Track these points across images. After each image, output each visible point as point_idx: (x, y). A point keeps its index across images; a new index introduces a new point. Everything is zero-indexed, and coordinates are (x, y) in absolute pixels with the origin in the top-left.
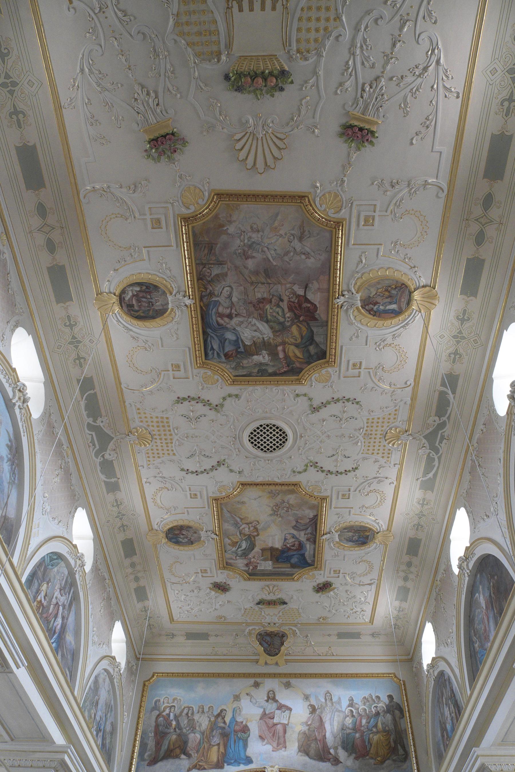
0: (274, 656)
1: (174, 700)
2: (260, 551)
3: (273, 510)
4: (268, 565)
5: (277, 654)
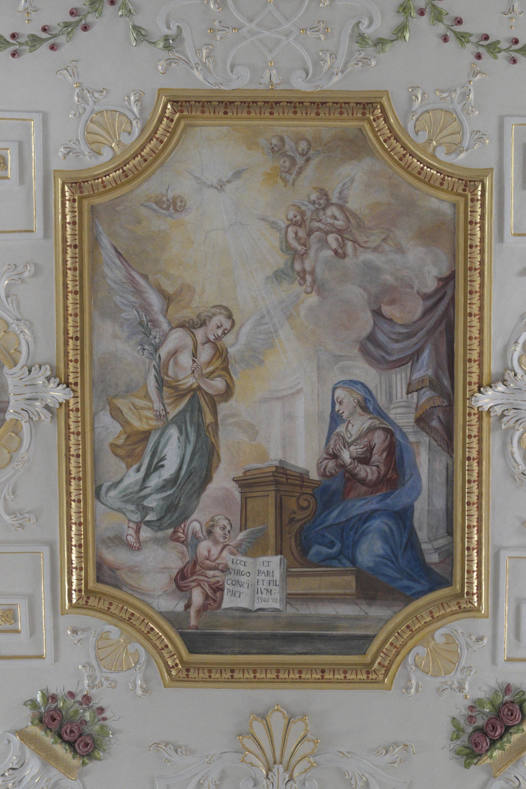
3: (287, 248)
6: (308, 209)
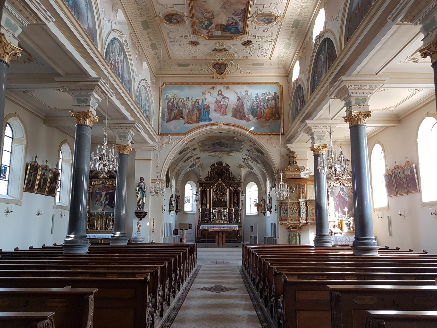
0: (221, 74)
1: (175, 95)
2: (215, 26)
4: (219, 33)
5: (223, 74)
6: (225, 2)
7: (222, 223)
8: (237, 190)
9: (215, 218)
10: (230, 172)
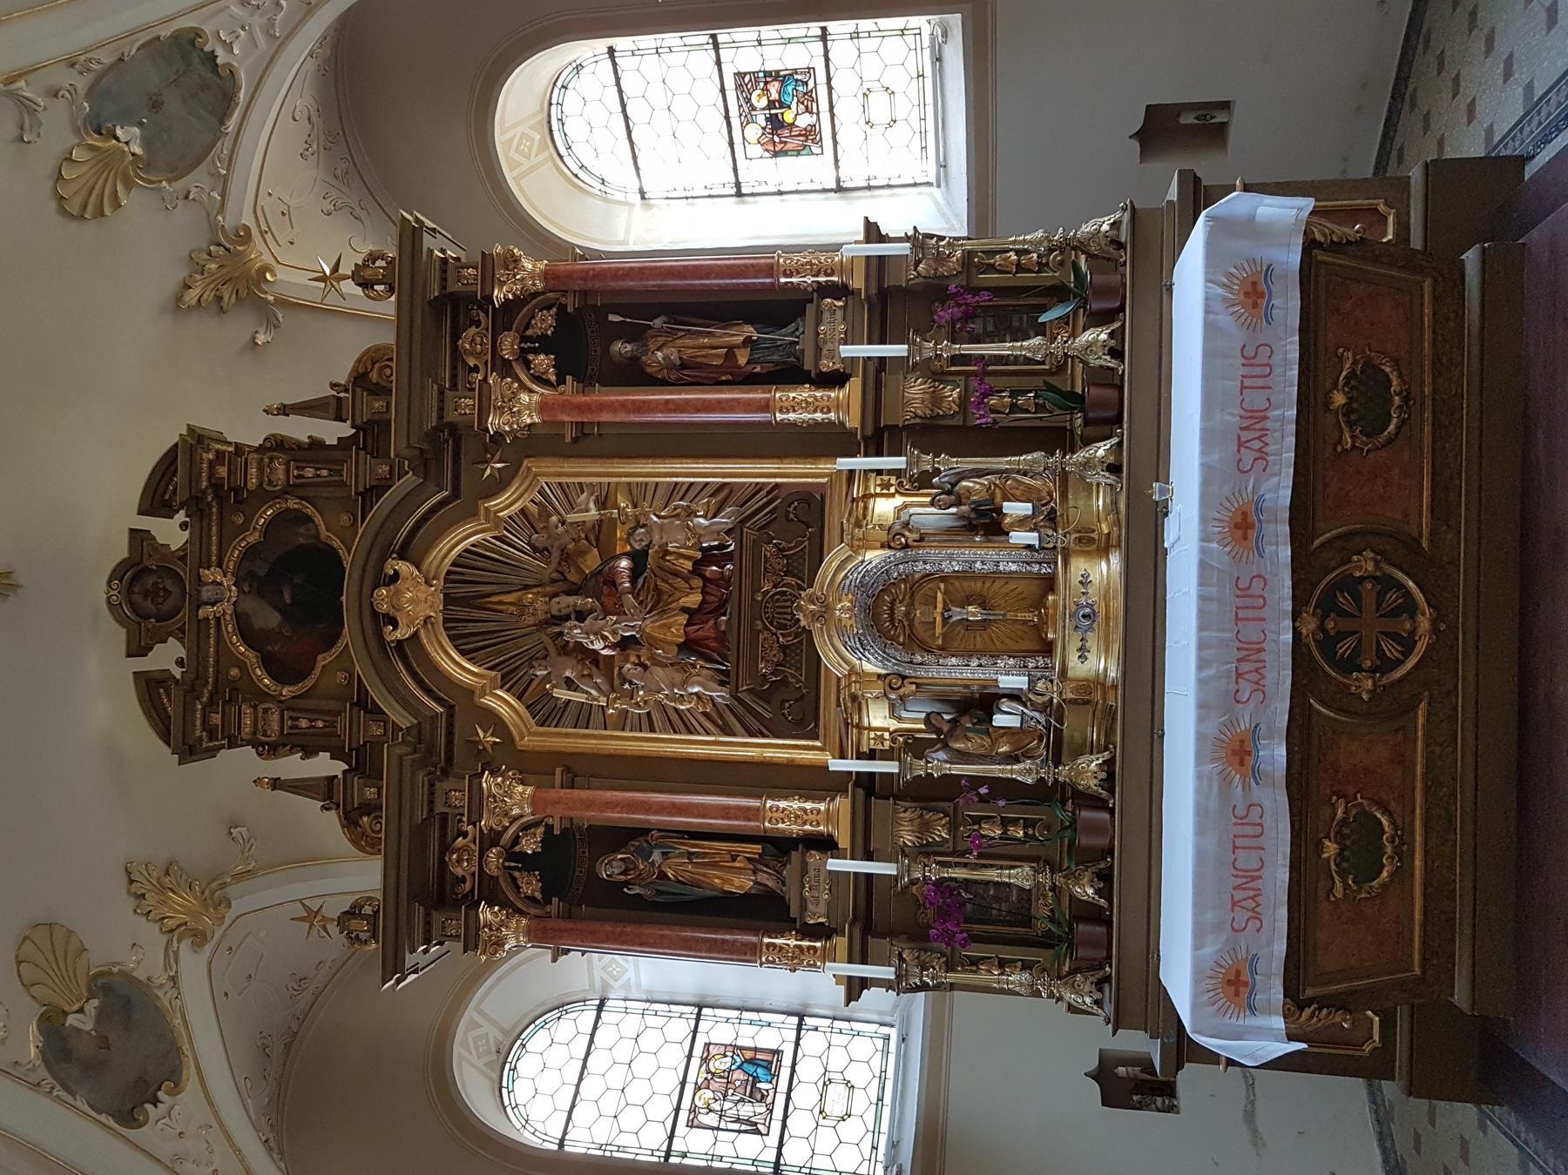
7: (1116, 560)
8: (545, 323)
9: (1014, 696)
10: (277, 445)
